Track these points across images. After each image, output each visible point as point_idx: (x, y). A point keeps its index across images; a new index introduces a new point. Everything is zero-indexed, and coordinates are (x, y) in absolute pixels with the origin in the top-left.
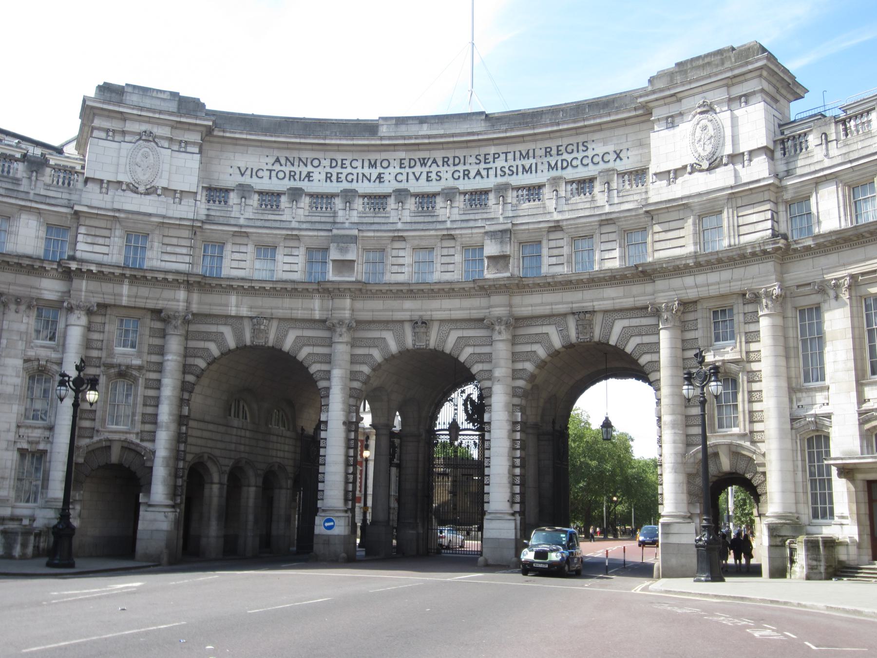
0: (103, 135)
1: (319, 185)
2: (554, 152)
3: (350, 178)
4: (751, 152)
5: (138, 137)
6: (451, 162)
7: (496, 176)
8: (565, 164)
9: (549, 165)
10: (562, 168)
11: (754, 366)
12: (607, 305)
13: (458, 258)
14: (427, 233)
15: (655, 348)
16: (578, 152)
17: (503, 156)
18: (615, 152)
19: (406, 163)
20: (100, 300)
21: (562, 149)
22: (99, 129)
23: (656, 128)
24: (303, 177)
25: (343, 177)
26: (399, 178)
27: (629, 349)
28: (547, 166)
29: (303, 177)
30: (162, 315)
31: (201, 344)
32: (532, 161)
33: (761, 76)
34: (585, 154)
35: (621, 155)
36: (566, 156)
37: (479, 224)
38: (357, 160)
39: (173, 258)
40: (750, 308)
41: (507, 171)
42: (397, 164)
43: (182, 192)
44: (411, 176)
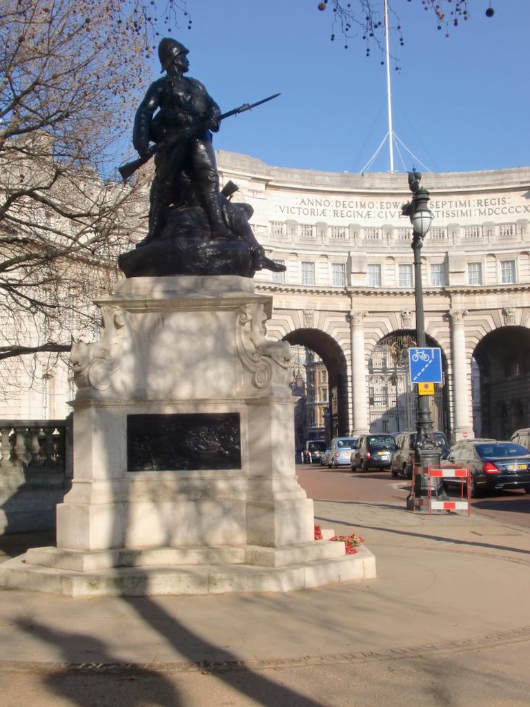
1: (331, 220)
2: (483, 203)
7: (443, 216)
8: (491, 212)
9: (480, 211)
10: (489, 215)
16: (499, 204)
17: (448, 204)
18: (524, 206)
19: (384, 205)
21: (489, 202)
24: (320, 213)
25: (345, 213)
28: (478, 212)
29: (319, 214)
31: (274, 328)
32: (468, 208)
34: (504, 206)
36: (491, 206)
37: (443, 250)
38: (352, 202)
42: (379, 205)
43: (258, 226)
44: (388, 214)
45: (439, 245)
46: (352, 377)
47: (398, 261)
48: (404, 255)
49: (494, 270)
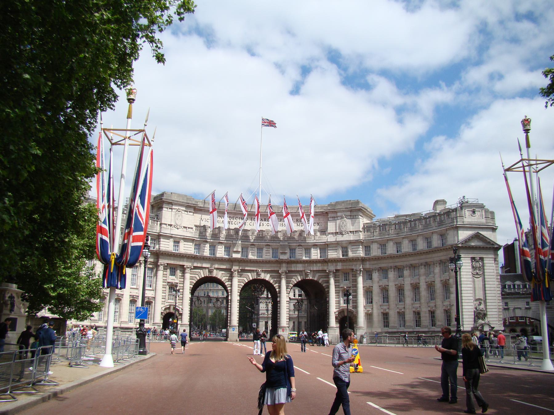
0: (166, 209)
2: (299, 221)
3: (235, 223)
4: (356, 231)
5: (176, 210)
6: (267, 220)
11: (355, 288)
12: (315, 269)
13: (271, 251)
14: (261, 244)
15: (328, 282)
20: (168, 262)
22: (165, 208)
23: (330, 219)
25: (233, 222)
26: (251, 224)
27: (320, 282)
30: (185, 267)
31: (194, 275)
33: (359, 211)
35: (319, 224)
39: (187, 249)
40: (354, 273)
41: (284, 225)
45: (276, 239)
46: (231, 300)
47: (257, 246)
48: (259, 244)
49: (301, 252)
